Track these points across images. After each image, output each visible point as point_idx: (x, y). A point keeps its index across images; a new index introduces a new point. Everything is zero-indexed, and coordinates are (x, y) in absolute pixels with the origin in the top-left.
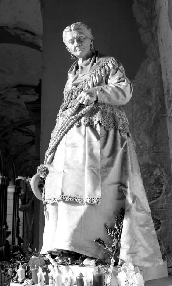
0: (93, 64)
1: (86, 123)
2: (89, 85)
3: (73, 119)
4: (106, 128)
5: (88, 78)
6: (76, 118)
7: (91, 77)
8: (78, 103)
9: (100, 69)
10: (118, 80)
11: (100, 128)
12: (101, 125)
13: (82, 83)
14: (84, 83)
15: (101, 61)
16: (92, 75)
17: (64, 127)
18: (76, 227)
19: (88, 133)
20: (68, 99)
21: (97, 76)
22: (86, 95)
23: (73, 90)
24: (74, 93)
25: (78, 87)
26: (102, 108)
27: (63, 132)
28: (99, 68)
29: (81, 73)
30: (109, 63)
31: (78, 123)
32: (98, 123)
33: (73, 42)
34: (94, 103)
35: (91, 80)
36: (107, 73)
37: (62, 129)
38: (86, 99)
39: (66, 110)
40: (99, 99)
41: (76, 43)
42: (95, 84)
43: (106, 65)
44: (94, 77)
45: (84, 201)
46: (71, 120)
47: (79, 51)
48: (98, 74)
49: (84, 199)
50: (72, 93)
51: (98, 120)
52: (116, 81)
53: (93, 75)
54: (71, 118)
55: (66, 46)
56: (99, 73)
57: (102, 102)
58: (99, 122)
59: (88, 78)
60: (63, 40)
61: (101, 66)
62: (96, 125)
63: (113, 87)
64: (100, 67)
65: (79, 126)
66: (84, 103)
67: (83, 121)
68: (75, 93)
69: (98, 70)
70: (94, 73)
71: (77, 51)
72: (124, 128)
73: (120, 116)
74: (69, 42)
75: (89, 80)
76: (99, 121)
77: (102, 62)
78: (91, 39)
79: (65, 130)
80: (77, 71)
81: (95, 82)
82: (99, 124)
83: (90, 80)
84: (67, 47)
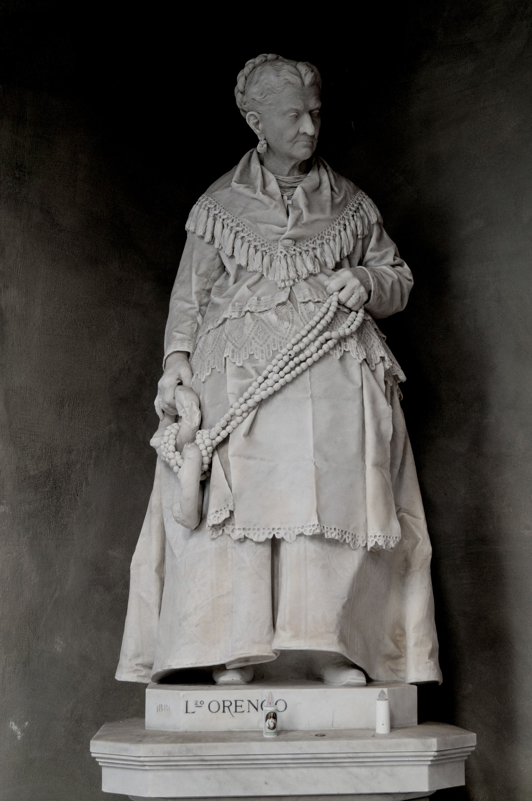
2: (334, 252)
10: (394, 260)
14: (319, 242)
17: (307, 353)
18: (346, 599)
20: (292, 275)
22: (359, 286)
27: (303, 365)
28: (351, 213)
35: (337, 239)
37: (302, 357)
39: (291, 306)
43: (360, 208)
44: (343, 233)
45: (357, 540)
47: (305, 147)
49: (358, 536)
51: (381, 355)
64: (351, 210)
66: (349, 304)
69: (351, 218)
70: (342, 222)
71: (297, 144)
75: (331, 238)
79: (309, 361)
80: (285, 198)
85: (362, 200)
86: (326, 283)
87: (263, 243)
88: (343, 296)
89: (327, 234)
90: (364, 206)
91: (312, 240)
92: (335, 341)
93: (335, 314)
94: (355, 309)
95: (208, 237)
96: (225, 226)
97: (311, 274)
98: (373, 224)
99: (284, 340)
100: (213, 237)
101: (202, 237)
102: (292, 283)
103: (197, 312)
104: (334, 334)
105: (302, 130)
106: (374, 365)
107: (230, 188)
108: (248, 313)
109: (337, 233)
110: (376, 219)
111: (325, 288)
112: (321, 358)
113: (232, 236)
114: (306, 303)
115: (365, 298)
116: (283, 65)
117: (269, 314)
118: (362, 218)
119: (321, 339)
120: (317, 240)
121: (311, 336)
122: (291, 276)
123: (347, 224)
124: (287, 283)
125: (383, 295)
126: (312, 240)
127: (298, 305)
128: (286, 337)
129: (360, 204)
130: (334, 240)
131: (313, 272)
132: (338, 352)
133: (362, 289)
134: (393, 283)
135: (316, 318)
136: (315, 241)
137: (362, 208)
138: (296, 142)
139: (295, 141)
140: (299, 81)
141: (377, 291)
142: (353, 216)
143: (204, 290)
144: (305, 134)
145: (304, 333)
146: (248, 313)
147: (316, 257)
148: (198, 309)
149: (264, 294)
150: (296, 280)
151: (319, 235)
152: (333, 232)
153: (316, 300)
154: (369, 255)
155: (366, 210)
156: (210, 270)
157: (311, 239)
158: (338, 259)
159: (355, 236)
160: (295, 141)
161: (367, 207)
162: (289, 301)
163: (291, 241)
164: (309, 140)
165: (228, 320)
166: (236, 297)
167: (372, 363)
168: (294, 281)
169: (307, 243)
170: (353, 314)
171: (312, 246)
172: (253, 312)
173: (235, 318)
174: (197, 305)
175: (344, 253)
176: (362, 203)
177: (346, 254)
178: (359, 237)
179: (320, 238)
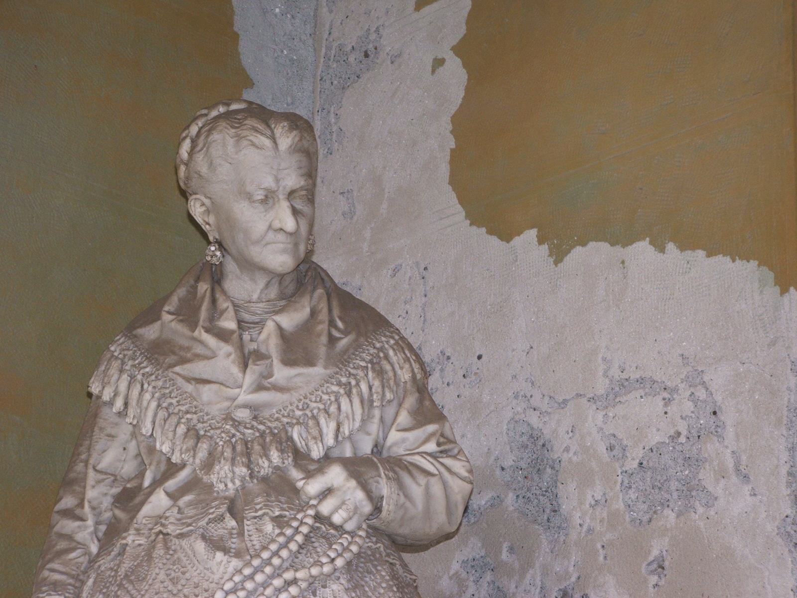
30: (394, 350)
34: (364, 526)
35: (333, 409)
39: (233, 523)
43: (381, 355)
47: (284, 251)
52: (431, 447)
53: (342, 391)
54: (289, 575)
64: (364, 360)
66: (337, 519)
71: (269, 247)
80: (246, 337)
85: (387, 342)
86: (300, 484)
87: (201, 414)
88: (325, 508)
89: (314, 399)
90: (391, 353)
91: (288, 410)
92: (304, 585)
93: (307, 537)
94: (349, 526)
95: (119, 404)
96: (146, 386)
97: (277, 468)
98: (405, 382)
99: (213, 585)
100: (126, 404)
101: (111, 403)
102: (238, 483)
103: (91, 533)
104: (300, 575)
105: (277, 225)
107: (159, 323)
108: (161, 536)
109: (333, 398)
110: (410, 375)
111: (297, 491)
113: (154, 404)
114: (260, 517)
115: (367, 508)
116: (246, 118)
117: (192, 538)
118: (380, 373)
119: (277, 582)
120: (295, 410)
121: (259, 578)
122: (237, 470)
123: (353, 382)
124: (230, 485)
125: (408, 504)
127: (246, 522)
128: (216, 577)
129: (381, 349)
130: (326, 411)
131: (280, 465)
133: (360, 495)
134: (427, 488)
135: (274, 547)
136: (294, 411)
137: (387, 357)
139: (264, 242)
140: (267, 142)
142: (367, 367)
143: (106, 494)
145: (247, 571)
146: (161, 536)
147: (290, 439)
148: (92, 529)
149: (190, 504)
150: (247, 478)
151: (300, 400)
152: (325, 397)
153: (277, 513)
154: (394, 436)
156: (120, 461)
158: (330, 441)
159: (367, 404)
161: (396, 354)
162: (228, 515)
163: (248, 411)
165: (128, 548)
166: (146, 510)
168: (243, 479)
169: (276, 415)
170: (345, 540)
171: (285, 420)
172: (168, 534)
173: (140, 545)
174: (90, 522)
176: (386, 346)
177: (347, 433)
178: (375, 404)
179: (301, 407)
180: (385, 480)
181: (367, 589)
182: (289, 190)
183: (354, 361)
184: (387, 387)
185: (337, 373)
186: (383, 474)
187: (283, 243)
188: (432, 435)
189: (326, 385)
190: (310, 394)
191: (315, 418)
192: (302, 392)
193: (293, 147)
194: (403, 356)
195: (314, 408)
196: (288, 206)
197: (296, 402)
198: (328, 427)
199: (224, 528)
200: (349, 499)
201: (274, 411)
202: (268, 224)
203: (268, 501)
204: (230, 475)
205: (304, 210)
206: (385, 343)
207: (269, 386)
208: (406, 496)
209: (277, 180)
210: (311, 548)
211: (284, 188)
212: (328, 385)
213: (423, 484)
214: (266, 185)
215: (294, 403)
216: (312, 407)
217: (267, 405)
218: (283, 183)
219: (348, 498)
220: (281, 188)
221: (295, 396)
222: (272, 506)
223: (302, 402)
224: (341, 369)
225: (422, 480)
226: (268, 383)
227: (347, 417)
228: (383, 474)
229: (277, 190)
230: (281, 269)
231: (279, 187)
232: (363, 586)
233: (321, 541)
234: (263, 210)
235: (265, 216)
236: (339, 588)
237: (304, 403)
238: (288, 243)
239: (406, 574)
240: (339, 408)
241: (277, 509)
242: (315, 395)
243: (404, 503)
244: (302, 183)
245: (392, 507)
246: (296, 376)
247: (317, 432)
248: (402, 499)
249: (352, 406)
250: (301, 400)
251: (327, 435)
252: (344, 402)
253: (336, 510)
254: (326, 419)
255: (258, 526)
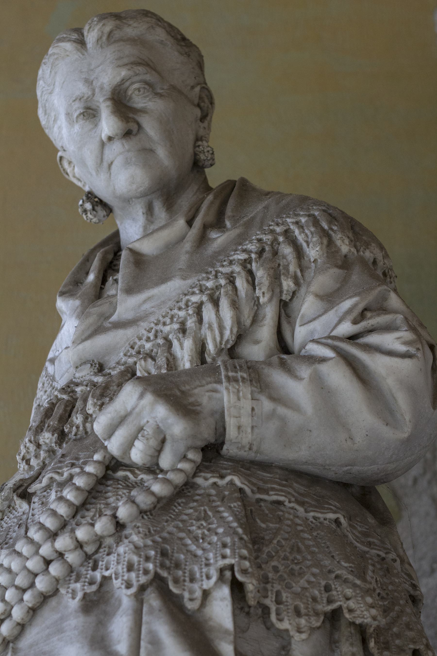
0: (202, 240)
1: (138, 579)
3: (61, 555)
4: (273, 617)
5: (172, 318)
6: (80, 545)
7: (190, 312)
8: (97, 457)
9: (248, 261)
11: (234, 615)
12: (237, 588)
13: (132, 348)
15: (253, 218)
16: (195, 299)
19: (155, 642)
21: (224, 304)
23: (78, 389)
24: (79, 404)
25: (107, 371)
26: (248, 490)
29: (130, 291)
31: (91, 583)
32: (221, 578)
33: (90, 113)
35: (190, 323)
36: (287, 284)
38: (149, 430)
39: (25, 506)
40: (231, 433)
41: (108, 124)
42: (211, 347)
43: (281, 239)
46: (48, 562)
48: (235, 289)
50: (70, 408)
51: (221, 563)
52: (346, 328)
53: (205, 298)
55: (57, 151)
56: (241, 283)
57: (251, 455)
58: (228, 574)
59: (172, 318)
60: (40, 112)
61: (253, 247)
62: (206, 594)
63: (323, 360)
65: (97, 603)
67: (122, 567)
68: (85, 401)
69: (237, 268)
71: (113, 167)
72: (398, 617)
73: (369, 544)
74: (68, 115)
76: (231, 568)
77: (262, 223)
78: (198, 106)
81: (214, 339)
82: (225, 591)
83: (183, 323)
84: (59, 154)
90: (297, 232)
98: (315, 261)
102: (43, 454)
106: (198, 594)
112: (33, 611)
126: (136, 347)
130: (183, 330)
132: (78, 585)
133: (161, 412)
138: (110, 165)
139: (105, 164)
140: (68, 46)
141: (246, 404)
144: (110, 139)
151: (149, 331)
152: (182, 314)
153: (66, 475)
155: (301, 238)
157: (132, 348)
160: (105, 164)
162: (15, 498)
164: (127, 147)
167: (191, 592)
175: (210, 351)
176: (292, 227)
178: (261, 300)
179: (152, 338)
180: (225, 384)
181: (189, 542)
182: (108, 88)
183: (231, 258)
184: (283, 274)
185: (203, 279)
186: (223, 377)
187: (121, 154)
188: (350, 311)
189: (185, 299)
190: (164, 317)
191: (169, 344)
192: (153, 319)
193: (104, 38)
194: (313, 229)
195: (169, 333)
196: (107, 106)
197: (145, 333)
198: (182, 348)
199: (16, 517)
200: (148, 422)
201: (122, 354)
202: (98, 139)
203: (60, 462)
204: (32, 448)
205: (148, 107)
206: (290, 224)
207: (110, 325)
208: (272, 399)
209: (89, 82)
210: (102, 506)
211: (102, 88)
212: (187, 297)
213: (306, 376)
214: (78, 93)
215: (143, 335)
216: (166, 332)
217: (110, 350)
218: (97, 84)
219: (145, 420)
220: (97, 90)
221: (142, 329)
222: (60, 468)
223: (153, 331)
224: (207, 273)
225: (305, 372)
226: (110, 323)
227: (210, 327)
228: (223, 377)
229: (93, 95)
230: (134, 187)
231: (93, 90)
232: (181, 539)
233: (120, 493)
234: (91, 126)
235: (96, 132)
236: (127, 549)
237: (157, 331)
238: (128, 151)
239: (312, 514)
240: (200, 321)
241: (65, 469)
242: (169, 316)
243: (274, 410)
244: (124, 73)
245: (246, 421)
246: (145, 301)
247: (164, 359)
248: (267, 405)
249: (218, 311)
250: (152, 328)
251: (182, 359)
252: (208, 313)
253: (130, 445)
254: (179, 340)
255: (44, 500)
